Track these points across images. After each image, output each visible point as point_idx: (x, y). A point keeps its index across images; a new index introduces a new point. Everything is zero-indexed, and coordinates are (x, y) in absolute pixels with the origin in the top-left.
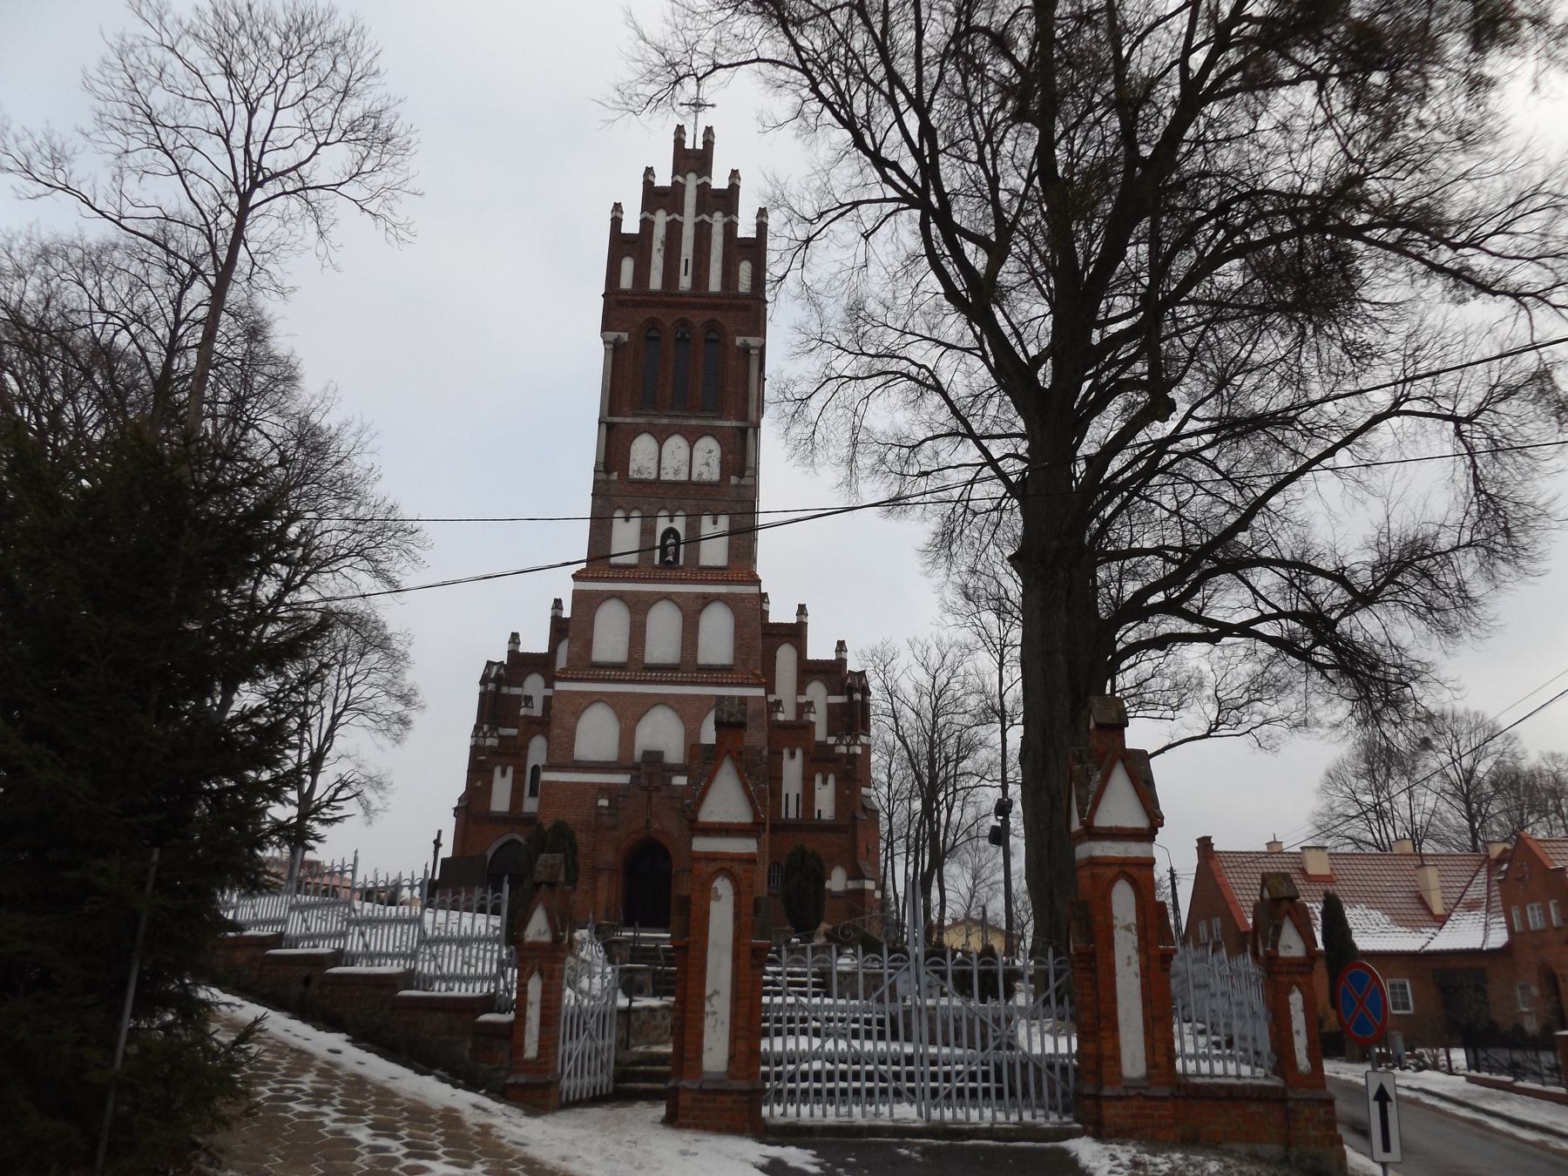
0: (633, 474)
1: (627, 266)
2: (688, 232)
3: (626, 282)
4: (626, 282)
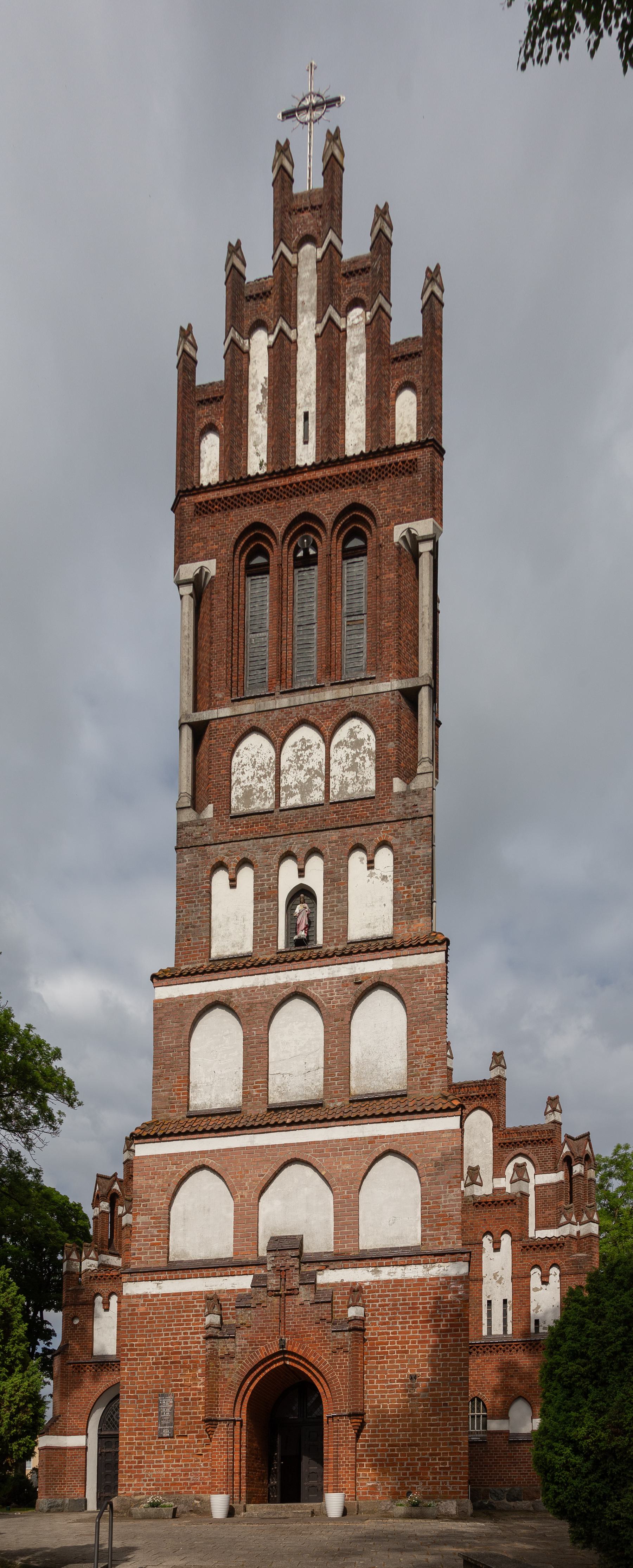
0: (237, 806)
1: (211, 448)
2: (307, 358)
3: (210, 470)
4: (210, 470)
